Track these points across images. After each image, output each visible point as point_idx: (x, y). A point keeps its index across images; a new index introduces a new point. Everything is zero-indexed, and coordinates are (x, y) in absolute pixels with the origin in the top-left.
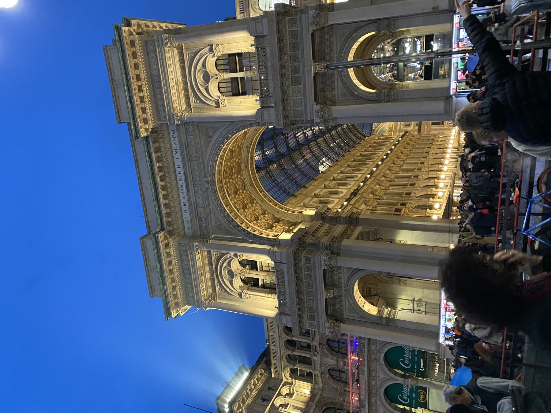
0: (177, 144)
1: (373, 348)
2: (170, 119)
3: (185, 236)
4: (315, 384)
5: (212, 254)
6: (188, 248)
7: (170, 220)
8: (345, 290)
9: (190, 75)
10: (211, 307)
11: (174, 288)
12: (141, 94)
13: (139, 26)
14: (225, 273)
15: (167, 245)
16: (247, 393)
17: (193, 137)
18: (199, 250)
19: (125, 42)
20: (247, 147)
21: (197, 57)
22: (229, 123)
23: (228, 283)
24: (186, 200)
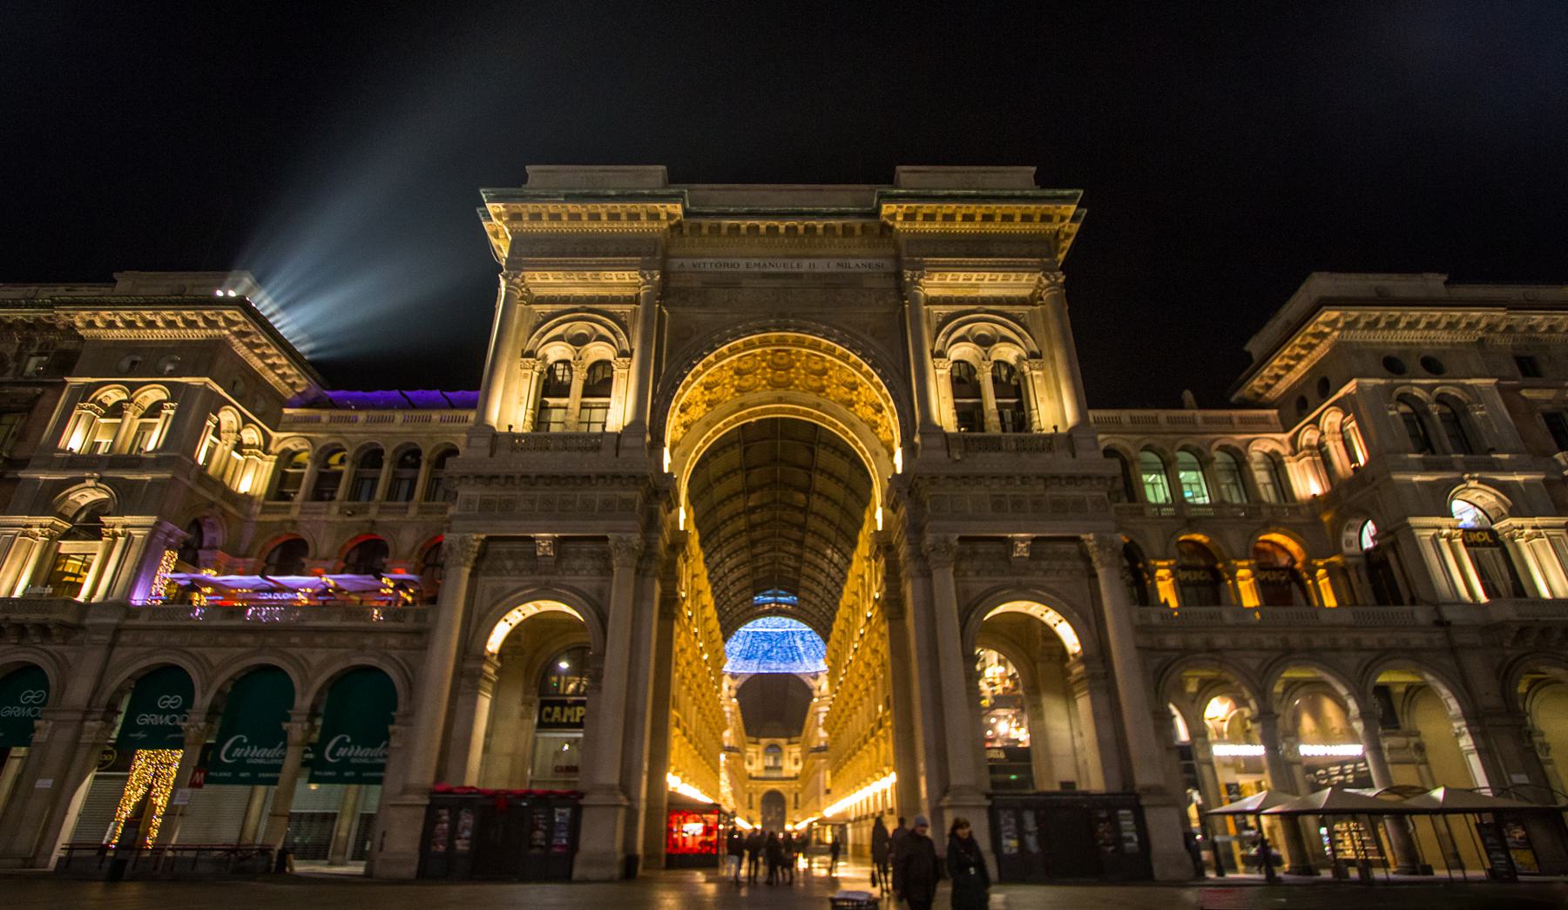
0: (857, 270)
1: (392, 641)
4: (264, 506)
5: (625, 306)
6: (647, 258)
7: (705, 231)
8: (547, 583)
9: (987, 312)
10: (507, 288)
11: (555, 217)
12: (959, 218)
13: (1068, 236)
14: (581, 328)
16: (258, 346)
18: (641, 280)
19: (1052, 206)
21: (1020, 329)
23: (559, 330)
24: (743, 268)
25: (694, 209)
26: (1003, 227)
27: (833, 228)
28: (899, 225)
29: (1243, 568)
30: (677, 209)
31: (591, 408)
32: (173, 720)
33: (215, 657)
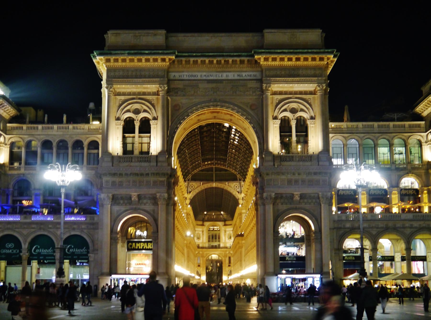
0: (245, 78)
1: (83, 227)
2: (267, 80)
3: (168, 72)
4: (10, 168)
6: (162, 79)
7: (184, 62)
9: (296, 98)
10: (108, 93)
11: (124, 60)
13: (332, 61)
15: (163, 60)
17: (251, 93)
20: (231, 120)
22: (261, 124)
24: (199, 78)
25: (179, 54)
26: (304, 63)
27: (236, 61)
28: (262, 62)
29: (395, 190)
30: (174, 57)
31: (142, 137)
32: (12, 251)
33: (25, 232)
